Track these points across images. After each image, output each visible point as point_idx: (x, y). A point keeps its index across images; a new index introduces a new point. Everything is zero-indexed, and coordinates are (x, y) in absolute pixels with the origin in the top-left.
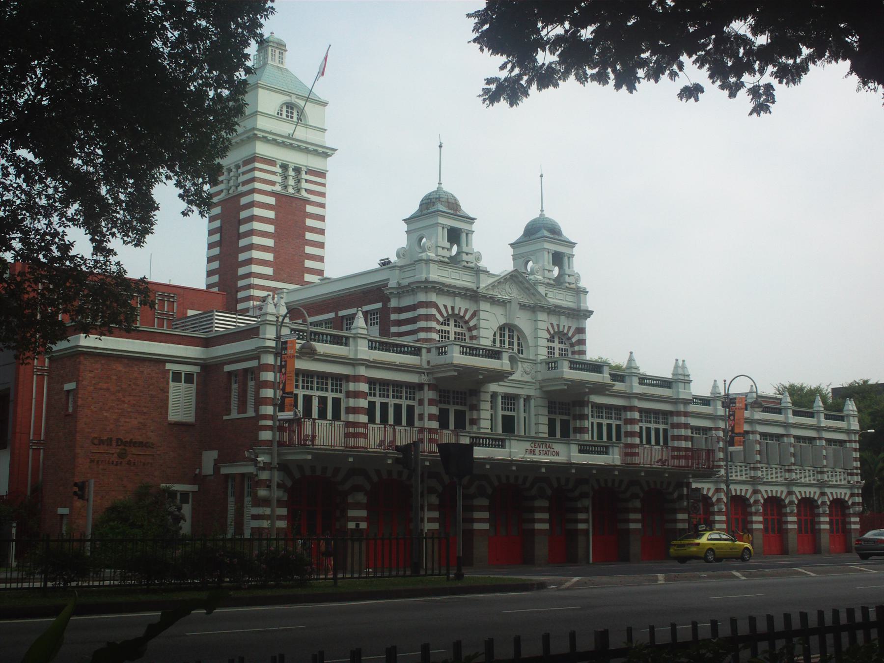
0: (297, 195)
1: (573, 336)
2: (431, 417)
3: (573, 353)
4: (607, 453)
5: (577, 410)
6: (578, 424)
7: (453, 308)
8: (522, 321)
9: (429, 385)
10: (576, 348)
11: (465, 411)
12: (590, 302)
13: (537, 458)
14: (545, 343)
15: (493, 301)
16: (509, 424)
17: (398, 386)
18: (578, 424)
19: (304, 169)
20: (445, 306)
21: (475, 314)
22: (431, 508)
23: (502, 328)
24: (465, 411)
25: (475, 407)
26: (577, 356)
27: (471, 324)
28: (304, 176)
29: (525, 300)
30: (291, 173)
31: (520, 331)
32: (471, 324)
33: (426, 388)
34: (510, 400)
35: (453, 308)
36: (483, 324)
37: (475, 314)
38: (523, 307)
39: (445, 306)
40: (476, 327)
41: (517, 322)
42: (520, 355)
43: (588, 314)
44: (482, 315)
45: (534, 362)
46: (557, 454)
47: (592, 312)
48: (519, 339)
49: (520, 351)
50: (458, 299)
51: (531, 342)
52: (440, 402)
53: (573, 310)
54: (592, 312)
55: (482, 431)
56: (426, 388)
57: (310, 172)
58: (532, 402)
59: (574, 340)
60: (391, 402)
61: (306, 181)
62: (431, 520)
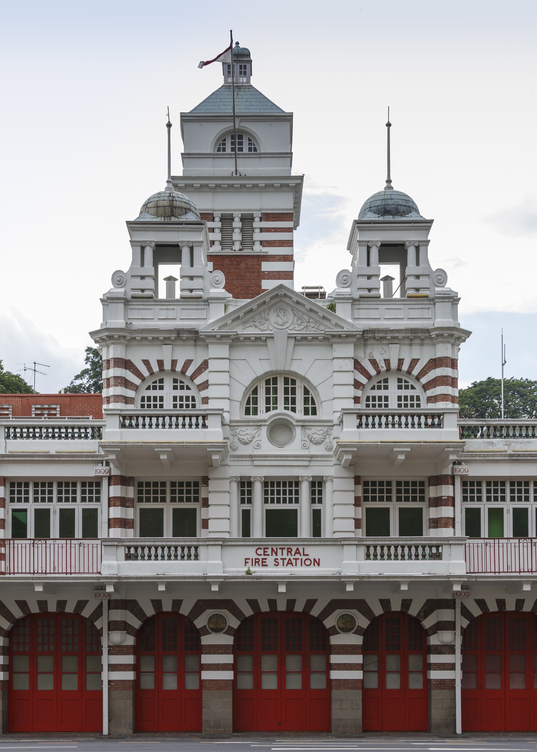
0: (247, 252)
1: (423, 373)
2: (124, 523)
3: (430, 399)
4: (438, 556)
5: (432, 492)
6: (434, 513)
7: (160, 363)
8: (309, 364)
9: (110, 478)
10: (430, 393)
11: (195, 510)
12: (465, 315)
13: (271, 570)
14: (351, 392)
15: (235, 342)
16: (281, 525)
17: (66, 486)
18: (434, 513)
19: (257, 215)
20: (146, 363)
21: (205, 365)
22: (114, 650)
23: (271, 380)
24: (195, 510)
25: (206, 503)
26: (431, 406)
27: (199, 380)
28: (257, 224)
29: (311, 331)
30: (237, 224)
31: (304, 379)
32: (199, 380)
33: (105, 483)
34: (281, 487)
35: (160, 363)
36: (213, 378)
37: (205, 365)
38: (301, 341)
39: (146, 363)
40: (205, 385)
41: (298, 368)
42: (310, 417)
43: (457, 336)
44: (212, 365)
45: (329, 425)
46: (317, 562)
47: (468, 333)
48: (306, 392)
49: (311, 408)
50: (167, 349)
51: (323, 393)
52: (140, 500)
53: (414, 331)
54: (468, 333)
55: (212, 536)
56: (105, 483)
57: (267, 217)
58: (328, 488)
59: (424, 380)
60: (55, 507)
61: (262, 230)
62: (113, 668)
